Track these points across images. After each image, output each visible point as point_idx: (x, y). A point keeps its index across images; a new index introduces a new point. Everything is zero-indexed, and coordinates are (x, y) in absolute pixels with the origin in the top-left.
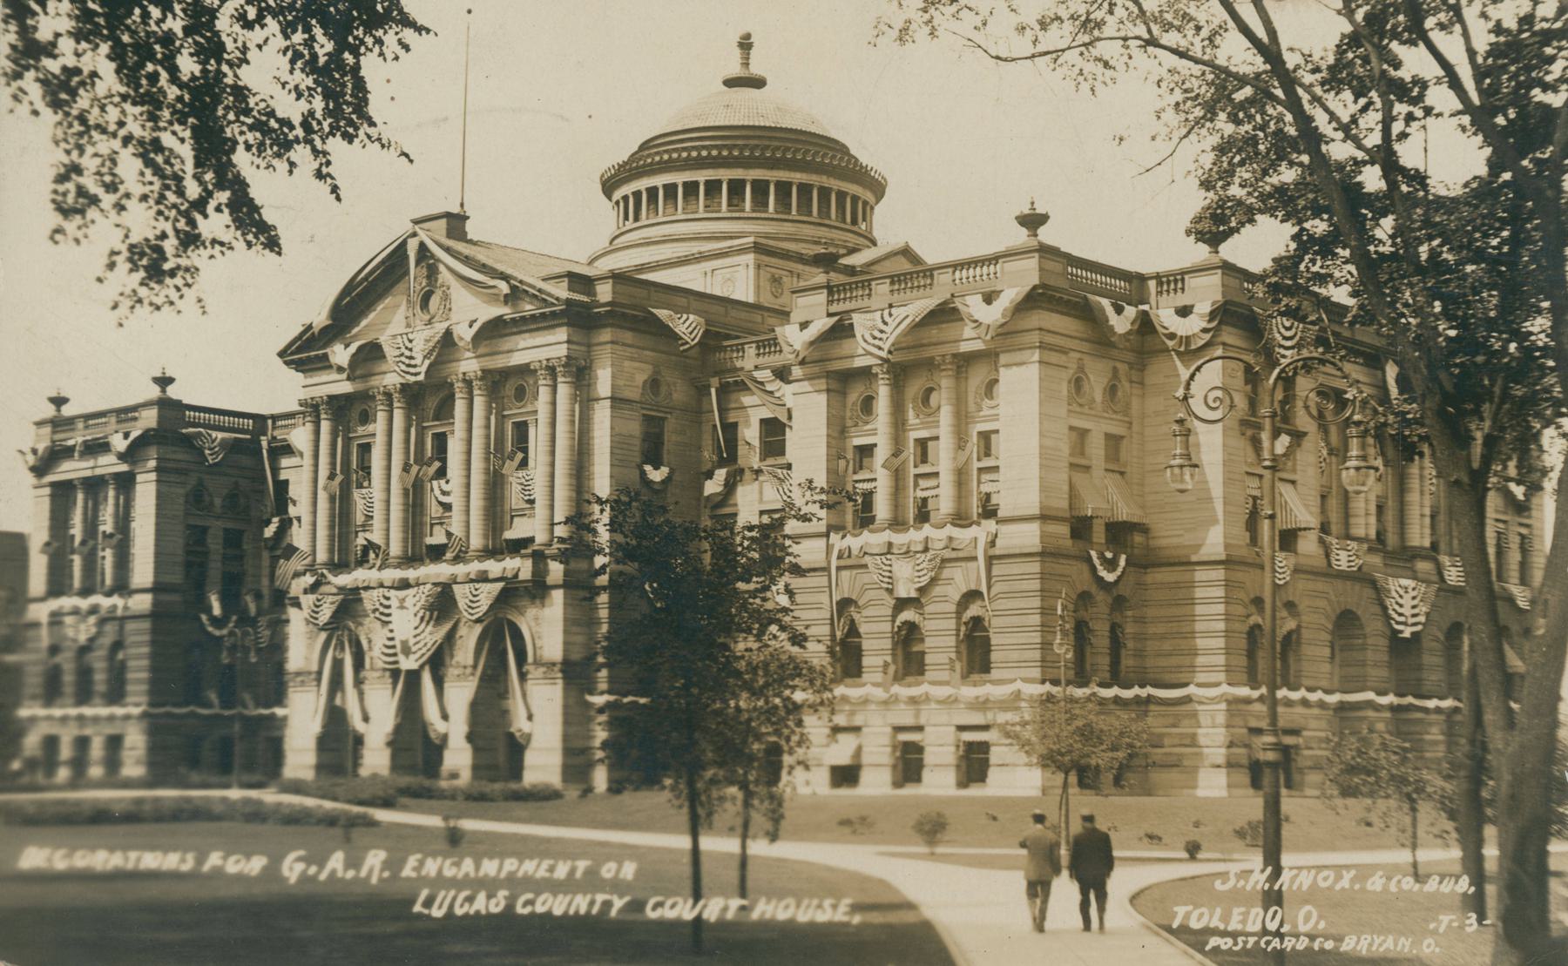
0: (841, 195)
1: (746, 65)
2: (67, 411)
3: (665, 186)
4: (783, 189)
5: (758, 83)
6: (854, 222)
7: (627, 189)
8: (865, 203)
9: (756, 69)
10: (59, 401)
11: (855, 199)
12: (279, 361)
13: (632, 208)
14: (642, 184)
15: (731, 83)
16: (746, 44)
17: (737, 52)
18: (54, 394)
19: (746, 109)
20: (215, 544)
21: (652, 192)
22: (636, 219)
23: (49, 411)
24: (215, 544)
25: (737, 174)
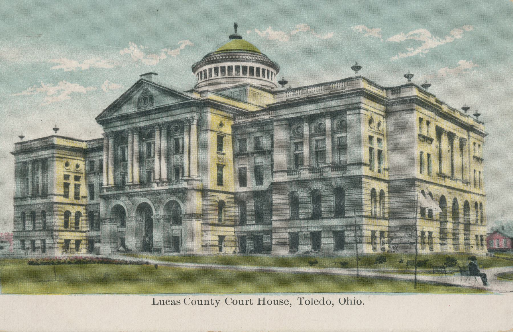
0: (268, 71)
1: (236, 32)
2: (24, 140)
3: (235, 66)
4: (252, 69)
5: (240, 37)
6: (272, 79)
7: (202, 69)
8: (274, 74)
9: (239, 33)
10: (22, 137)
11: (272, 73)
12: (96, 123)
13: (202, 75)
14: (207, 67)
15: (232, 37)
16: (236, 26)
17: (233, 28)
18: (20, 135)
19: (236, 44)
20: (72, 181)
21: (210, 70)
22: (201, 79)
23: (19, 140)
24: (72, 181)
25: (230, 64)
